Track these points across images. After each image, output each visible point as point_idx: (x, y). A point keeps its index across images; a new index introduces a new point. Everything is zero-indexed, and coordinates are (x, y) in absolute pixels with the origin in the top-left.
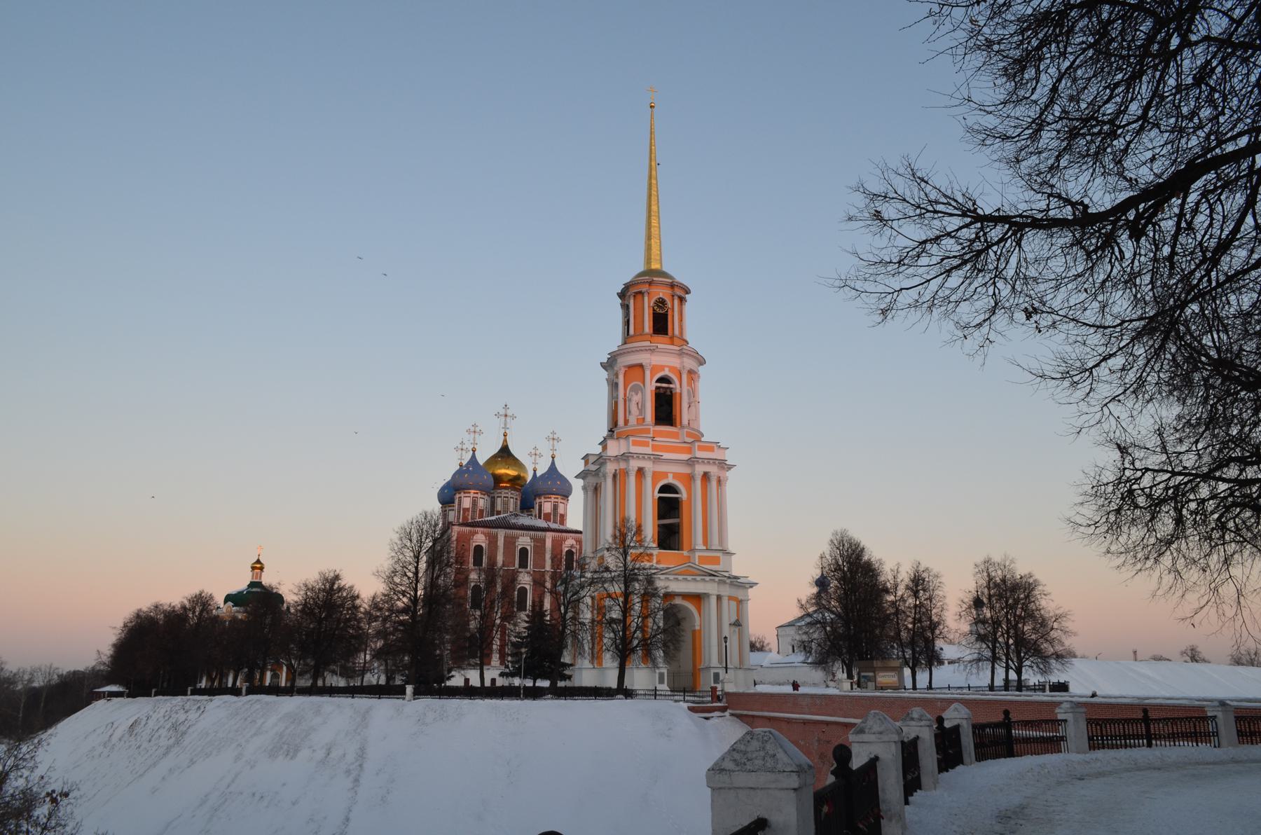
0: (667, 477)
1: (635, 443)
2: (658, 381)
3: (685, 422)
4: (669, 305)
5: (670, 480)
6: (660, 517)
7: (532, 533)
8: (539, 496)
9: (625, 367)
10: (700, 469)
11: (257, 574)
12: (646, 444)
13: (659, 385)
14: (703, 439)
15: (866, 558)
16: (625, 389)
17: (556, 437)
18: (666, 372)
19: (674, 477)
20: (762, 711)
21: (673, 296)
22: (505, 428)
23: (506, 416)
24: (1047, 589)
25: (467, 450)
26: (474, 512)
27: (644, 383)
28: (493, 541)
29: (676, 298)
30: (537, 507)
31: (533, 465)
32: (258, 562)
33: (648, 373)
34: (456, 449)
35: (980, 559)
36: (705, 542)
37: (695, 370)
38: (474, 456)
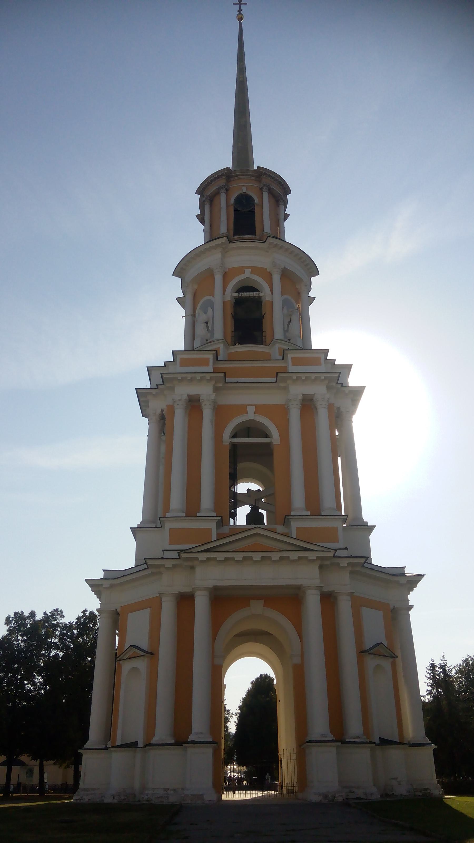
4: (256, 200)
5: (251, 415)
19: (256, 412)
21: (261, 189)
33: (218, 279)
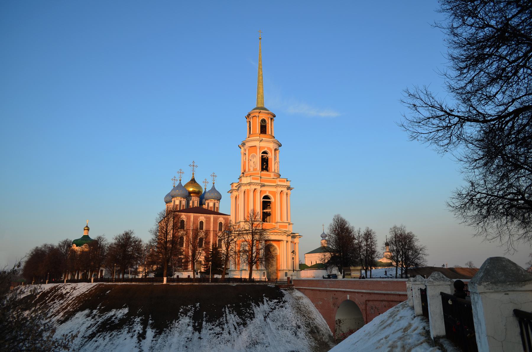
0: (266, 193)
1: (253, 179)
2: (262, 153)
3: (273, 170)
4: (267, 122)
5: (267, 194)
6: (263, 209)
7: (222, 216)
8: (208, 199)
9: (249, 147)
10: (280, 189)
11: (86, 232)
12: (257, 179)
13: (263, 155)
14: (280, 177)
15: (347, 226)
16: (249, 156)
17: (215, 175)
18: (266, 150)
19: (269, 193)
20: (309, 287)
22: (193, 171)
23: (194, 166)
24: (417, 238)
25: (177, 180)
26: (180, 206)
27: (257, 154)
28: (188, 218)
29: (270, 119)
30: (207, 204)
31: (206, 187)
32: (87, 227)
33: (258, 150)
34: (172, 179)
35: (392, 226)
36: (281, 219)
37: (278, 148)
38: (180, 183)
